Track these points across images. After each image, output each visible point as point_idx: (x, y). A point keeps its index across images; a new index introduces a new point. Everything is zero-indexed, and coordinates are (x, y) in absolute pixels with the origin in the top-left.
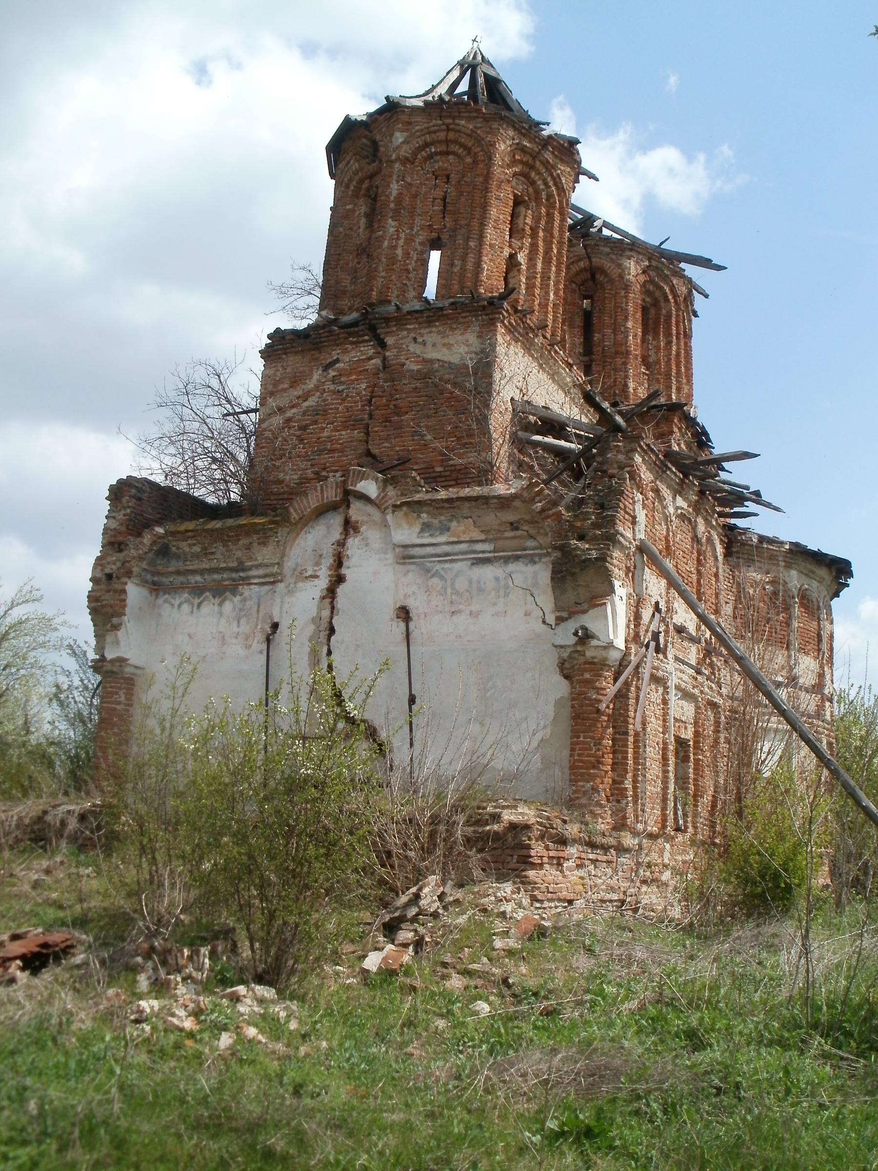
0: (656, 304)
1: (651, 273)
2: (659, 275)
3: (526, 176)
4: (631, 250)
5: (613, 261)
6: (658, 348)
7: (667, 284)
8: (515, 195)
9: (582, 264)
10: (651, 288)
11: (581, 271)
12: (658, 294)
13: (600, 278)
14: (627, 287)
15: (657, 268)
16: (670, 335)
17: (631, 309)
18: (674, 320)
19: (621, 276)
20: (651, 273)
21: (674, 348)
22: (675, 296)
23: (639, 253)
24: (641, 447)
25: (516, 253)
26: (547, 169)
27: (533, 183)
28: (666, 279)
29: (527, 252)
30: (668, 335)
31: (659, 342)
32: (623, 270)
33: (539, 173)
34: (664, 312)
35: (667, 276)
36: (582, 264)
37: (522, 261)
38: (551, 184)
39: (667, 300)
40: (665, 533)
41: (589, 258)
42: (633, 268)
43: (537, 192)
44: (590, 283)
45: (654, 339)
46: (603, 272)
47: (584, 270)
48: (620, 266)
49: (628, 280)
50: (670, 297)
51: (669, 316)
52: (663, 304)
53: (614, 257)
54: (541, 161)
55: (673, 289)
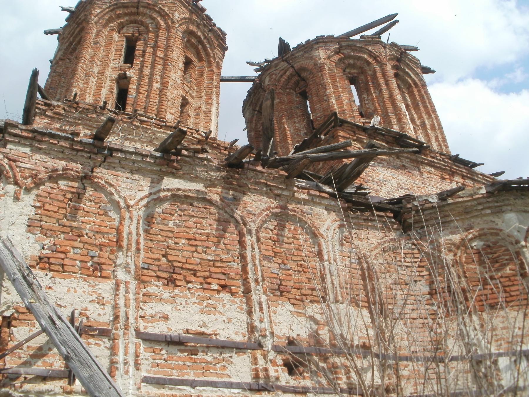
0: (363, 72)
1: (345, 52)
2: (353, 50)
3: (135, 22)
4: (317, 43)
5: (307, 58)
6: (373, 99)
7: (365, 53)
8: (128, 38)
9: (288, 73)
10: (351, 61)
11: (289, 78)
12: (359, 63)
13: (304, 75)
14: (321, 68)
15: (348, 46)
16: (379, 85)
17: (328, 80)
18: (379, 74)
19: (315, 64)
20: (345, 52)
21: (386, 94)
22: (375, 58)
23: (326, 42)
24: (16, 135)
25: (125, 74)
26: (150, 9)
27: (142, 23)
28: (361, 50)
29: (137, 68)
30: (378, 86)
31: (371, 94)
32: (315, 60)
33: (144, 15)
34: (370, 73)
35: (361, 47)
36: (288, 73)
37: (132, 75)
38: (155, 15)
39: (369, 63)
40: (116, 223)
41: (292, 67)
42: (321, 54)
43: (147, 27)
44: (302, 83)
45: (368, 95)
46: (303, 69)
47: (292, 75)
48: (312, 58)
49: (321, 63)
50: (371, 60)
51: (375, 72)
52: (367, 68)
53: (307, 55)
54: (143, 7)
55: (370, 54)
